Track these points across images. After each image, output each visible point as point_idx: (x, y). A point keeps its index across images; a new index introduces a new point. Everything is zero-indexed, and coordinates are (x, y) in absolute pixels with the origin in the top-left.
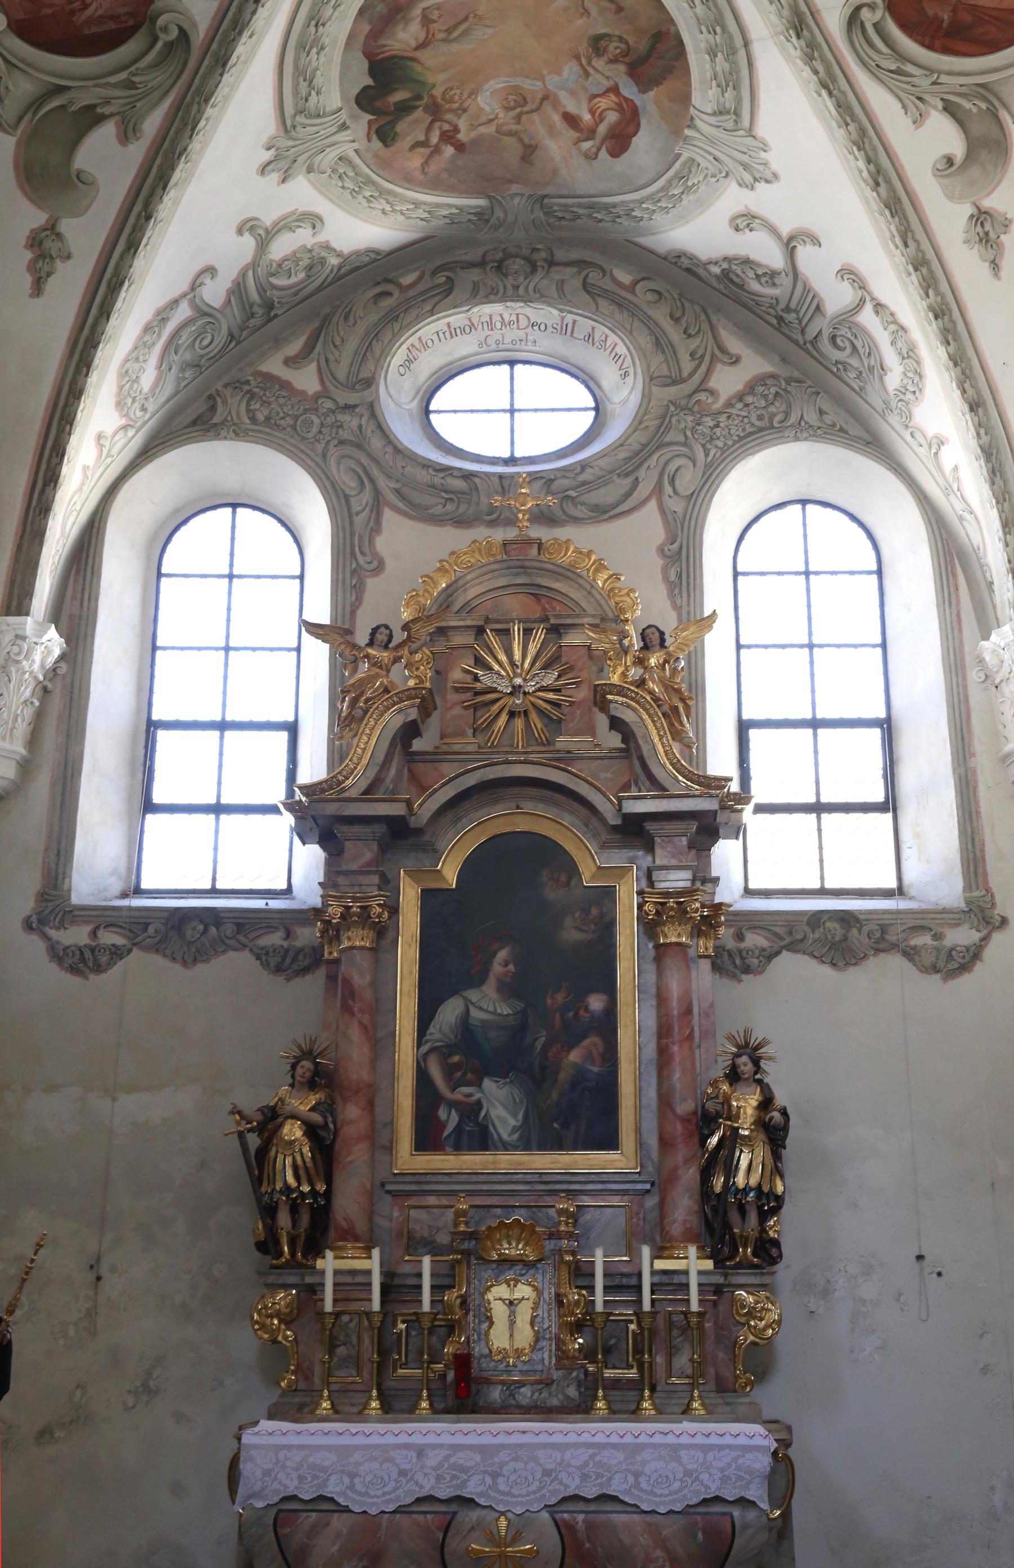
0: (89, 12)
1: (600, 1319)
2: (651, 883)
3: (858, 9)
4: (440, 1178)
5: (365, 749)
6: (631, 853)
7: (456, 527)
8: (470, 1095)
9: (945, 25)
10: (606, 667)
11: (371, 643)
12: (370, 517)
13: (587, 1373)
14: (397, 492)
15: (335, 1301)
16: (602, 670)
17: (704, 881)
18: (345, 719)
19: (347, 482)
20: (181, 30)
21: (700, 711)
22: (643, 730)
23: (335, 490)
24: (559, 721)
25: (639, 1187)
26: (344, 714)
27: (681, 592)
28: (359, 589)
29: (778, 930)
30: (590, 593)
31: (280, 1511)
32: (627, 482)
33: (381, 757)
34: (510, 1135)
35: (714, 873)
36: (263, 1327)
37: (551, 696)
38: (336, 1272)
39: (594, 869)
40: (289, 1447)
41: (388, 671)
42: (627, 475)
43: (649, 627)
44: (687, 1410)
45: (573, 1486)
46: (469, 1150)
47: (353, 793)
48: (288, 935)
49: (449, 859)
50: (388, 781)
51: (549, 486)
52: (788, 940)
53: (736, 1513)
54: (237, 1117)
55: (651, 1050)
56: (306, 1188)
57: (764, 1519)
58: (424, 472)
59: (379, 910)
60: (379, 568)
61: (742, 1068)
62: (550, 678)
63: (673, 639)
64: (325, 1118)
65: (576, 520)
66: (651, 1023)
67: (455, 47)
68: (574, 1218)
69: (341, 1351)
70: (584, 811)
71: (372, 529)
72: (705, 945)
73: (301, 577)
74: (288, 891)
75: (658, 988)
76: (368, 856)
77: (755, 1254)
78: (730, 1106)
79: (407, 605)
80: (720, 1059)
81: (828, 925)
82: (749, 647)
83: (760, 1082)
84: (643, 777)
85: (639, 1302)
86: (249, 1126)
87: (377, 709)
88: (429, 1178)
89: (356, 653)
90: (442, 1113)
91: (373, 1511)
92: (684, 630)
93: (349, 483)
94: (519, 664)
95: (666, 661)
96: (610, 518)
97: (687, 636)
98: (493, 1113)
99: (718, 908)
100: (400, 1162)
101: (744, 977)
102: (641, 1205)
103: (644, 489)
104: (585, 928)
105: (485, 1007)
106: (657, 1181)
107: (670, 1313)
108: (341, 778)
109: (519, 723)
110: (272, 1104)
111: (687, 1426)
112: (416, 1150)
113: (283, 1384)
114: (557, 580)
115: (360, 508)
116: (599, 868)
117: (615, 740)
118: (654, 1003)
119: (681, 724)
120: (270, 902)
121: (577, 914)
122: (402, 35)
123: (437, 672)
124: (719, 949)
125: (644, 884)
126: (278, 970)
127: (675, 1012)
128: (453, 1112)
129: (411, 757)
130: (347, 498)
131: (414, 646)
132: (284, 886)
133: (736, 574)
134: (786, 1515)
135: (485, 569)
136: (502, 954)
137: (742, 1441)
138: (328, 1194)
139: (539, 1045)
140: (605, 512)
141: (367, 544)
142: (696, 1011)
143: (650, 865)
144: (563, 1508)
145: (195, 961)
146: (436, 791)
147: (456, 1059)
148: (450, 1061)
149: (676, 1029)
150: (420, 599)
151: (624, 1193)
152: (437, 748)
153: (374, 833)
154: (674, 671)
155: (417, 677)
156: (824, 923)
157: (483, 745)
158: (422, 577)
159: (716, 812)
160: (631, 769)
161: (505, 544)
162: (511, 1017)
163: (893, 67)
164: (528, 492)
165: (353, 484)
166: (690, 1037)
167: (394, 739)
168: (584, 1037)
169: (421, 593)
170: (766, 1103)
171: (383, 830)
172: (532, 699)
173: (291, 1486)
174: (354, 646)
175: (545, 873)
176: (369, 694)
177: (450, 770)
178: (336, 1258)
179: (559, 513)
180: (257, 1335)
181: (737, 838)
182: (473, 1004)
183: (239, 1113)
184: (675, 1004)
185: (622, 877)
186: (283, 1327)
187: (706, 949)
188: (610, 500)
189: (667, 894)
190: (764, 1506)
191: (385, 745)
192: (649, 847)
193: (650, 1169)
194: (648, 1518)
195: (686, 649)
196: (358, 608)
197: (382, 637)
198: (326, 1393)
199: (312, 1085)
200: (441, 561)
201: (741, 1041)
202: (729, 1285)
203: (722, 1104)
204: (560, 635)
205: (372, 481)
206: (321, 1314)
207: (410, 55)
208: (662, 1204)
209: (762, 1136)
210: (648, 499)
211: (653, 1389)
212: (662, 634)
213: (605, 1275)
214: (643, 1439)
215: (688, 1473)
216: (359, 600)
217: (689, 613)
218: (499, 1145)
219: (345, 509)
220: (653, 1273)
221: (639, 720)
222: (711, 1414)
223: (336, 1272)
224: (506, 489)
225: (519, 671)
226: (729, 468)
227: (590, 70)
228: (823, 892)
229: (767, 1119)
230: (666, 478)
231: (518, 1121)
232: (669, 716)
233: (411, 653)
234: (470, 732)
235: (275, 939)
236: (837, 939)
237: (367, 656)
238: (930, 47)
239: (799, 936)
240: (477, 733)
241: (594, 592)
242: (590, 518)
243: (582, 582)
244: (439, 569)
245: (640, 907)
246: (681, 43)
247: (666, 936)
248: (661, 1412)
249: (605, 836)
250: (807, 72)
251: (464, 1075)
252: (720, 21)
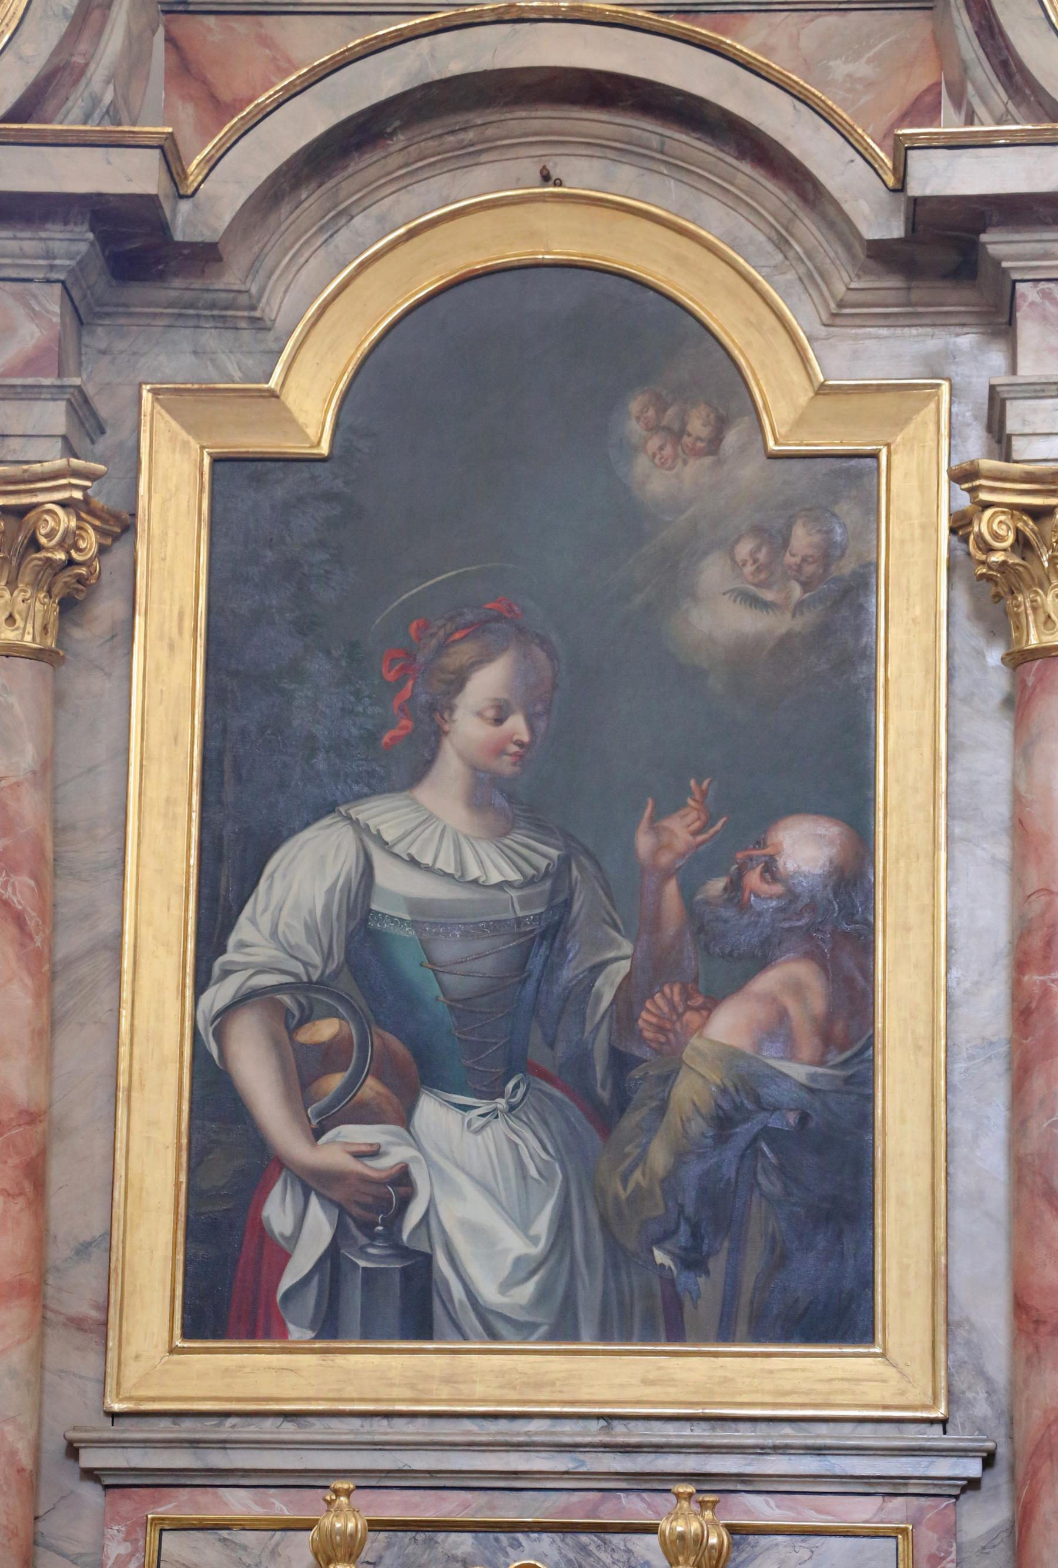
4: (268, 1429)
8: (375, 1152)
25: (943, 1467)
34: (506, 1286)
39: (804, 395)
46: (365, 1336)
49: (306, 354)
50: (98, 74)
59: (66, 521)
75: (1018, 799)
84: (982, 72)
88: (228, 1429)
98: (450, 1214)
100: (132, 1373)
102: (951, 1532)
104: (769, 596)
105: (427, 860)
106: (1002, 1452)
112: (186, 1335)
118: (1002, 850)
121: (744, 549)
139: (607, 988)
143: (1002, 379)
147: (325, 1030)
148: (305, 1036)
153: (49, 255)
162: (514, 894)
168: (761, 961)
171: (83, 247)
175: (634, 406)
182: (384, 844)
185: (900, 422)
193: (982, 1409)
218: (470, 1320)
231: (534, 1240)
245: (960, 525)
251: (352, 1084)
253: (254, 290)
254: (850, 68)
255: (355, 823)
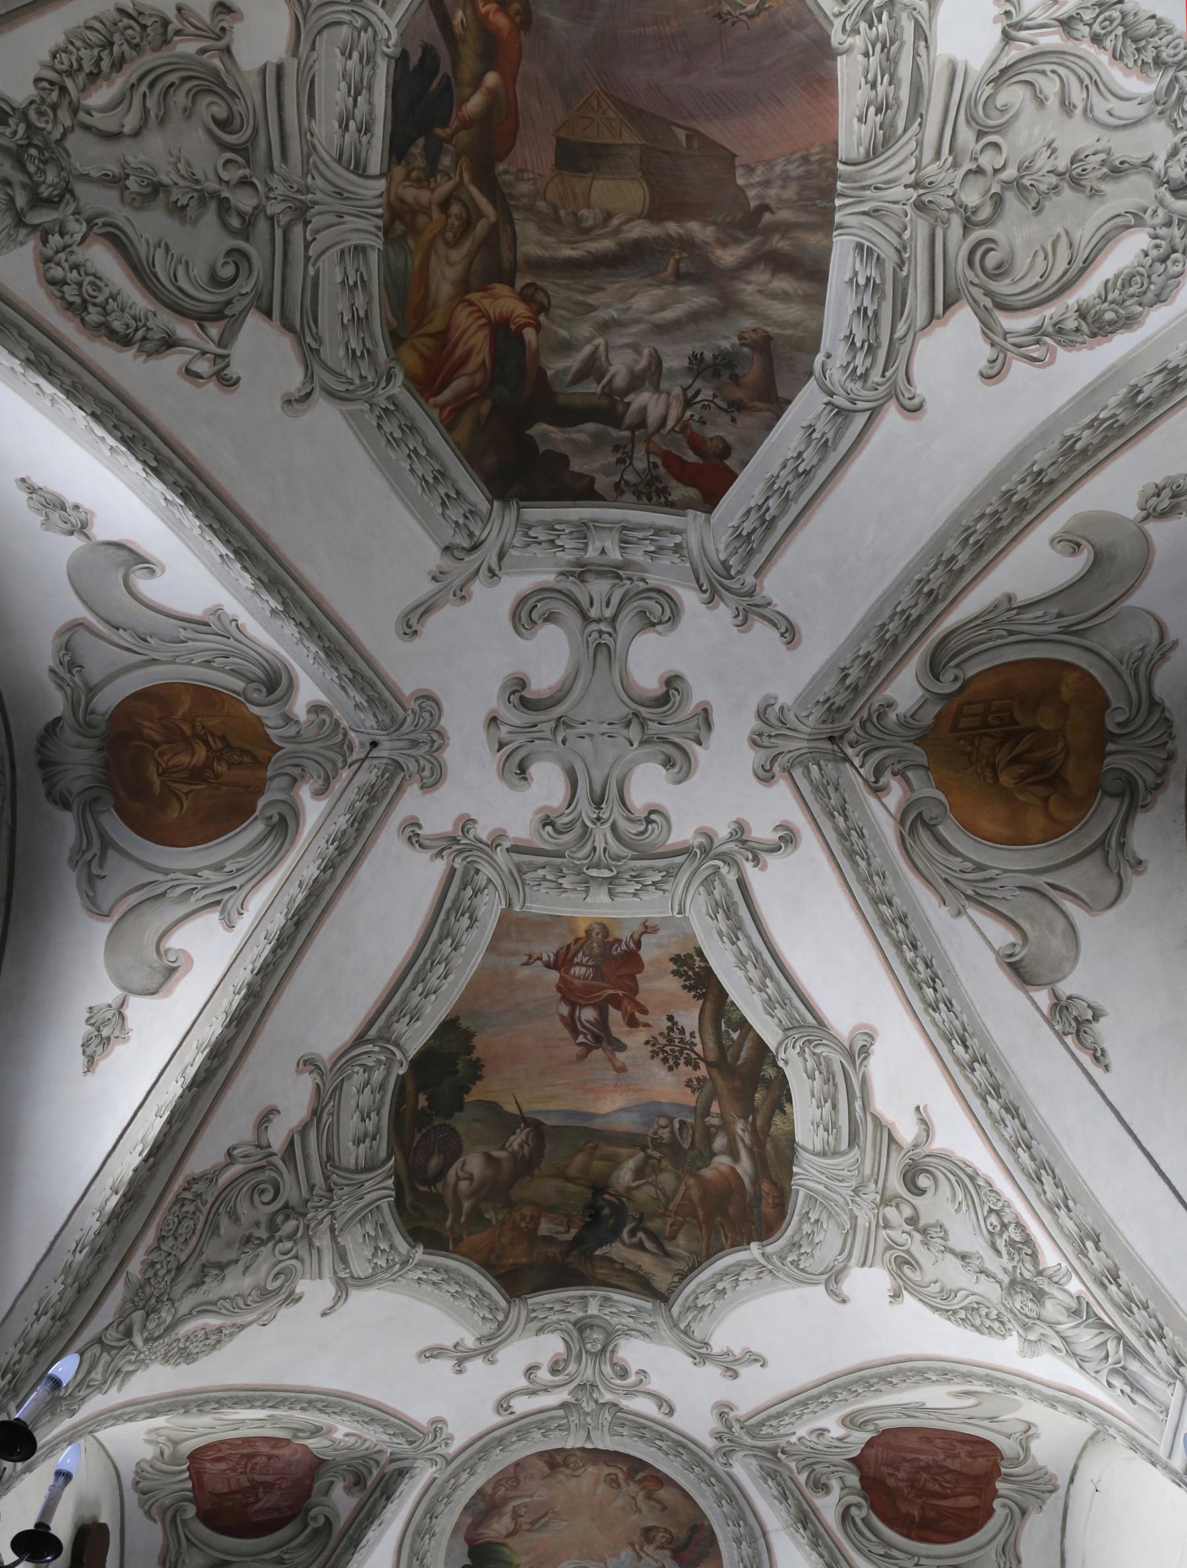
0: (259, 1505)
3: (848, 1507)
9: (917, 1519)
20: (327, 1520)
67: (536, 1536)
122: (496, 1526)
163: (882, 1552)
207: (500, 1541)
227: (643, 1554)
238: (908, 1536)
246: (713, 1534)
250: (815, 1556)
252: (742, 1516)
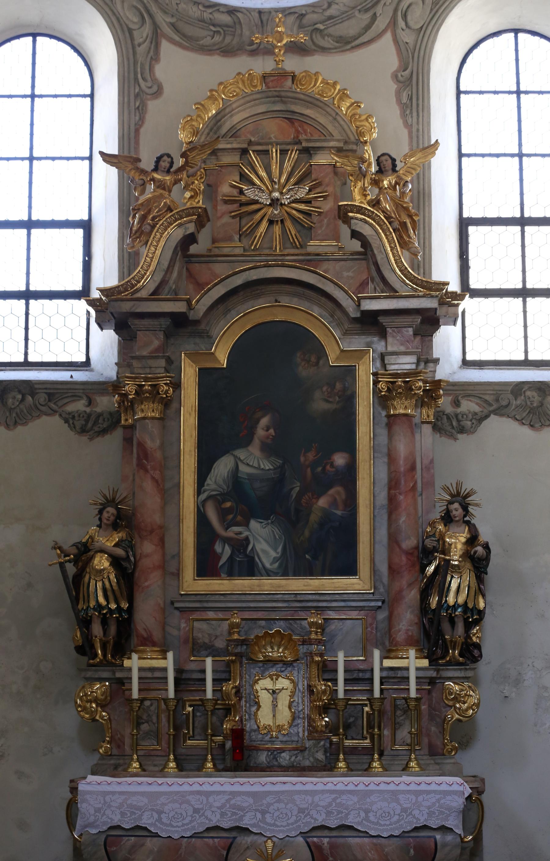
1: (341, 704)
2: (384, 366)
4: (217, 598)
5: (153, 258)
6: (369, 339)
7: (223, 56)
8: (240, 533)
10: (348, 181)
11: (156, 169)
12: (150, 48)
13: (331, 743)
14: (173, 26)
15: (140, 690)
16: (345, 184)
17: (427, 362)
18: (136, 232)
19: (130, 17)
21: (427, 215)
22: (378, 242)
23: (121, 25)
24: (311, 228)
25: (373, 604)
26: (135, 228)
27: (411, 113)
28: (141, 110)
29: (487, 397)
30: (335, 119)
31: (108, 836)
32: (367, 17)
33: (166, 264)
34: (271, 564)
35: (435, 356)
36: (84, 709)
37: (302, 207)
38: (140, 669)
39: (338, 352)
40: (113, 793)
41: (170, 191)
42: (367, 10)
43: (383, 155)
44: (406, 768)
45: (320, 820)
46: (239, 576)
47: (144, 294)
48: (90, 403)
49: (220, 344)
50: (171, 282)
51: (301, 20)
52: (495, 406)
53: (438, 837)
54: (58, 551)
55: (382, 498)
56: (113, 606)
57: (459, 840)
58: (195, 8)
59: (166, 388)
60: (158, 92)
61: (454, 512)
62: (302, 193)
63: (403, 164)
64: (127, 552)
65: (324, 50)
66: (383, 475)
68: (322, 628)
69: (145, 727)
70: (330, 304)
71: (152, 58)
72: (428, 413)
73: (92, 96)
74: (87, 364)
75: (389, 449)
76: (156, 343)
77: (461, 655)
78: (444, 542)
79: (184, 129)
80: (438, 505)
81: (528, 393)
82: (469, 155)
83: (468, 523)
84: (377, 279)
85: (371, 691)
86: (67, 558)
87: (162, 225)
88: (207, 598)
89: (144, 178)
90: (218, 548)
91: (176, 836)
92: (411, 156)
93: (133, 18)
94: (276, 180)
95: (396, 183)
96: (353, 48)
97: (414, 161)
98: (258, 547)
99: (437, 384)
100: (185, 585)
101: (459, 436)
102: (374, 618)
103: (381, 23)
104: (331, 400)
105: (251, 464)
106: (387, 600)
107: (395, 699)
108: (134, 282)
109: (277, 229)
110: (84, 541)
111: (406, 779)
112: (197, 576)
113: (101, 751)
114: (308, 108)
115: (141, 40)
116: (342, 351)
117: (356, 245)
118: (386, 460)
119: (409, 237)
120: (74, 374)
121: (325, 389)
123: (209, 185)
124: (439, 415)
125: (378, 364)
126: (83, 431)
127: (402, 469)
128: (227, 547)
129: (188, 258)
130: (130, 31)
131: (191, 171)
132: (83, 359)
133: (459, 93)
134: (478, 839)
135: (247, 99)
136: (264, 421)
137: (444, 787)
138: (130, 610)
139: (294, 494)
140: (348, 43)
141: (147, 71)
142: (419, 466)
143: (383, 350)
144: (313, 834)
145: (16, 423)
146: (210, 289)
147: (228, 504)
148: (223, 506)
149: (403, 482)
150: (194, 123)
151: (361, 608)
152: (210, 250)
153: (161, 325)
154: (403, 194)
155: (193, 190)
156: (524, 392)
157: (247, 247)
158: (195, 105)
159: (436, 309)
160: (368, 268)
161: (264, 77)
162: (272, 472)
164: (283, 30)
165: (135, 20)
166: (414, 488)
167: (176, 247)
168: (331, 487)
169: (194, 117)
170: (472, 540)
171: (168, 323)
172: (288, 210)
173: (116, 820)
174: (143, 172)
175: (298, 355)
176: (155, 213)
177: (221, 270)
178: (140, 658)
179: (310, 44)
180: (80, 715)
181: (455, 324)
182: (239, 459)
183: (60, 548)
184: (401, 462)
185: (361, 358)
186: (99, 709)
187: (428, 416)
188: (352, 32)
189: (396, 375)
190: (459, 831)
191: (169, 254)
192: (383, 334)
193: (382, 590)
194: (375, 840)
195: (413, 172)
196: (141, 126)
197: (165, 164)
198: (135, 757)
199: (115, 526)
200: (211, 91)
201: (454, 491)
202: (440, 678)
203: (438, 541)
204: (310, 156)
205: (151, 16)
206: (130, 700)
208: (390, 617)
209: (469, 565)
210: (384, 32)
211: (381, 754)
212: (394, 160)
213: (346, 671)
214: (372, 787)
215: (404, 810)
216: (142, 120)
217: (418, 130)
218: (263, 572)
219: (129, 41)
220: (382, 669)
221: (374, 233)
222: (424, 771)
223: (140, 669)
224: (265, 22)
225: (277, 186)
226: (452, 5)
228: (527, 363)
229: (472, 553)
230: (399, 13)
231: (278, 553)
232: (399, 230)
233: (188, 177)
234: (237, 237)
235: (80, 406)
236: (535, 405)
237: (153, 179)
239: (504, 403)
240: (243, 237)
241: (338, 118)
242: (336, 48)
243: (329, 110)
244: (209, 98)
245: (376, 383)
247: (395, 408)
248: (386, 770)
249: (347, 326)
251: (235, 517)
253: (208, 329)
254: (348, 274)
255: (234, 456)
